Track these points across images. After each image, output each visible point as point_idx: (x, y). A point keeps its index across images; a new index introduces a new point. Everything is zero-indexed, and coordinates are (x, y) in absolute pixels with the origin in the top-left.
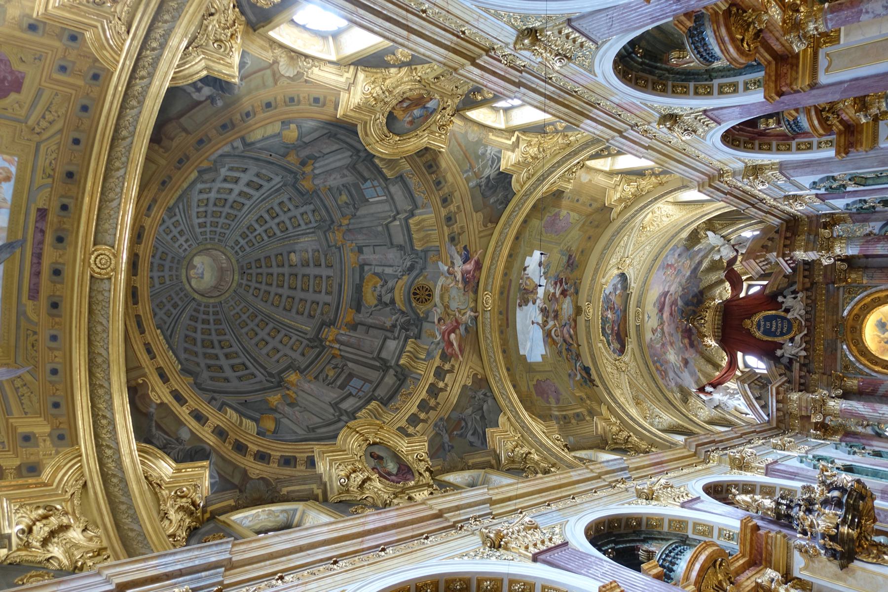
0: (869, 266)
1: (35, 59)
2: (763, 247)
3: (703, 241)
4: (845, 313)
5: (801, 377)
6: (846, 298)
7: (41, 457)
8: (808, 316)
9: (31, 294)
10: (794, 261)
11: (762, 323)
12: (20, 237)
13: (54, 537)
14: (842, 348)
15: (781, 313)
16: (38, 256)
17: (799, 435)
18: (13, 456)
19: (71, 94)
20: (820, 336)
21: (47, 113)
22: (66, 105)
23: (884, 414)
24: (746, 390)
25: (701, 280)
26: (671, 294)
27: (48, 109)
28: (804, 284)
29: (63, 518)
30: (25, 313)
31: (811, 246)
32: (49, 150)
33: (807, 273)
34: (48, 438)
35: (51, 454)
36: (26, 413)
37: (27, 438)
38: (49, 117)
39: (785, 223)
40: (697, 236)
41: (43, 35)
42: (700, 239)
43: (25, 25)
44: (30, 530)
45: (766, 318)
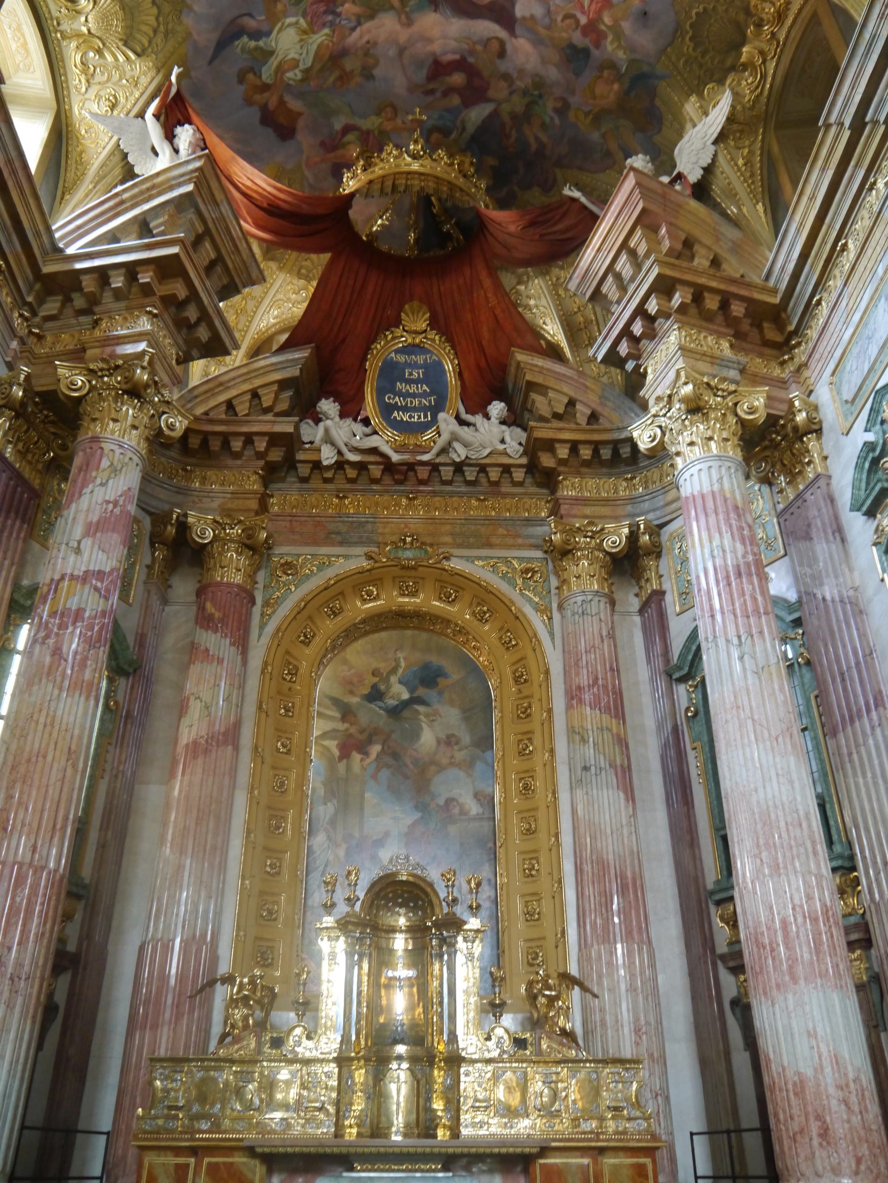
0: (615, 617)
2: (688, 244)
4: (455, 564)
5: (249, 439)
6: (506, 561)
8: (447, 472)
10: (636, 356)
11: (420, 359)
14: (346, 557)
17: (14, 344)
20: (387, 508)
23: (78, 551)
24: (172, 188)
26: (502, 53)
28: (549, 445)
31: (703, 366)
33: (586, 453)
39: (777, 300)
40: (711, 81)
42: (700, 95)
45: (433, 374)
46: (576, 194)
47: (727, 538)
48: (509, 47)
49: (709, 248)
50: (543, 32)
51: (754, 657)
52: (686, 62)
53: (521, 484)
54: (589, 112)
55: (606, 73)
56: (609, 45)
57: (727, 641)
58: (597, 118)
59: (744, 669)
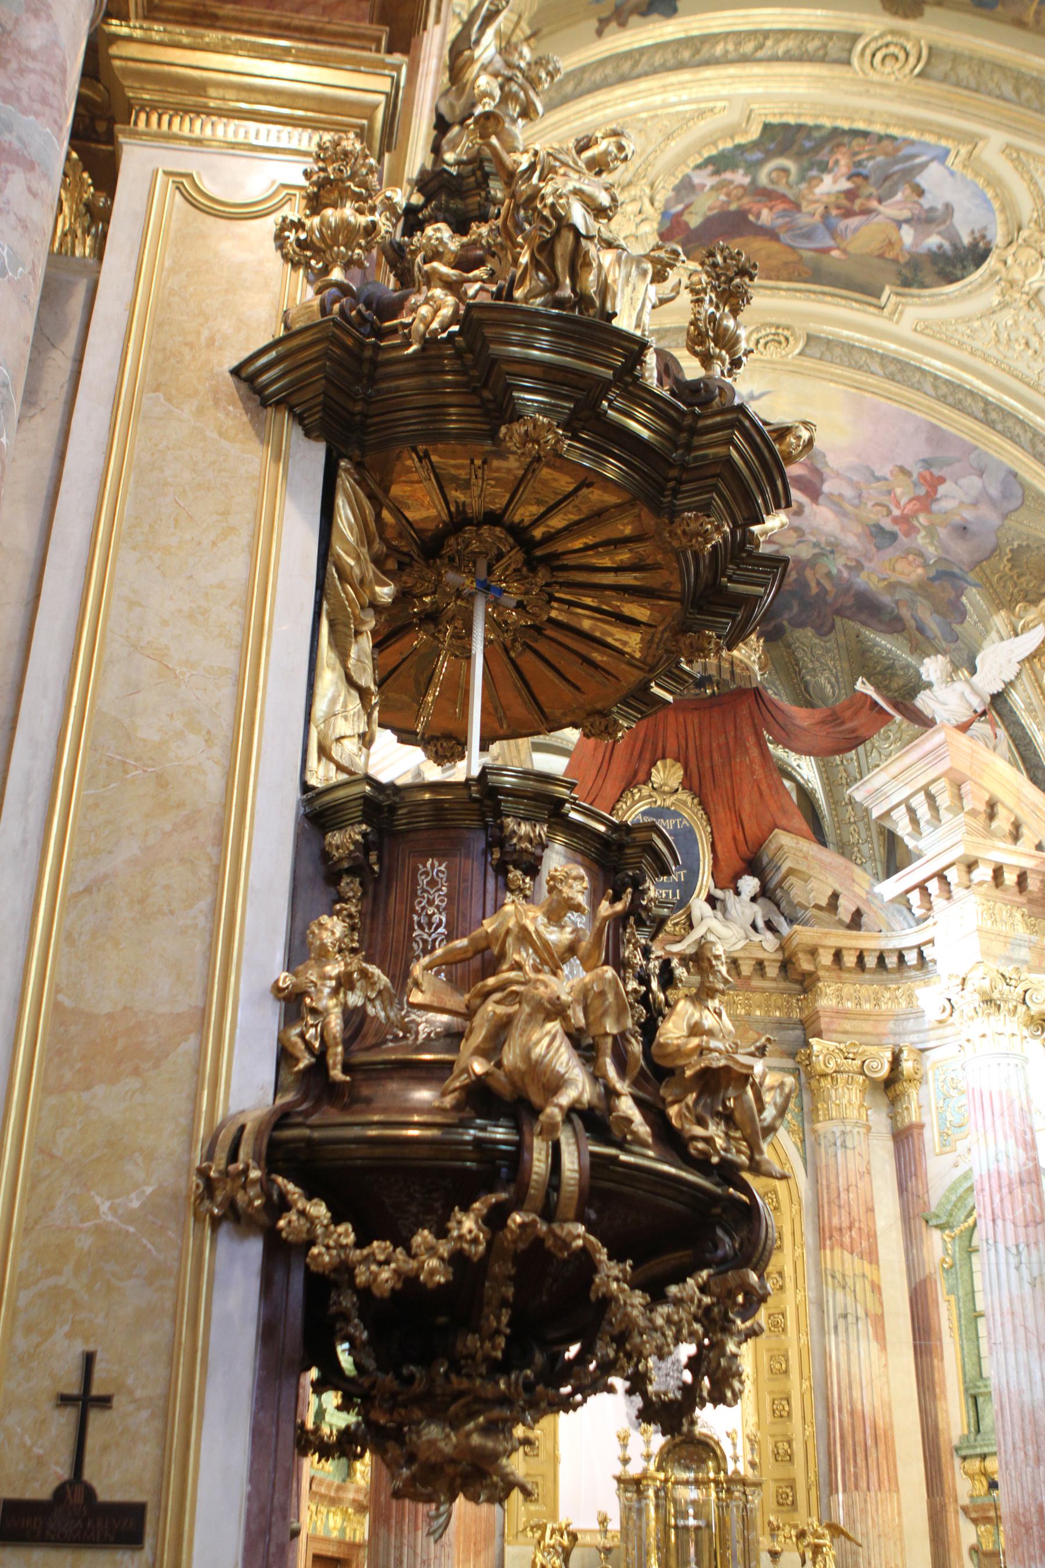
3: (1000, 620)
15: (705, 881)
25: (824, 630)
33: (850, 960)
42: (1011, 610)
46: (870, 691)
47: (1012, 1141)
48: (807, 510)
49: (1011, 811)
50: (849, 508)
51: (1030, 1269)
52: (1001, 578)
53: (774, 980)
54: (884, 579)
55: (911, 557)
56: (921, 539)
57: (1007, 1248)
58: (892, 587)
59: (1021, 1279)
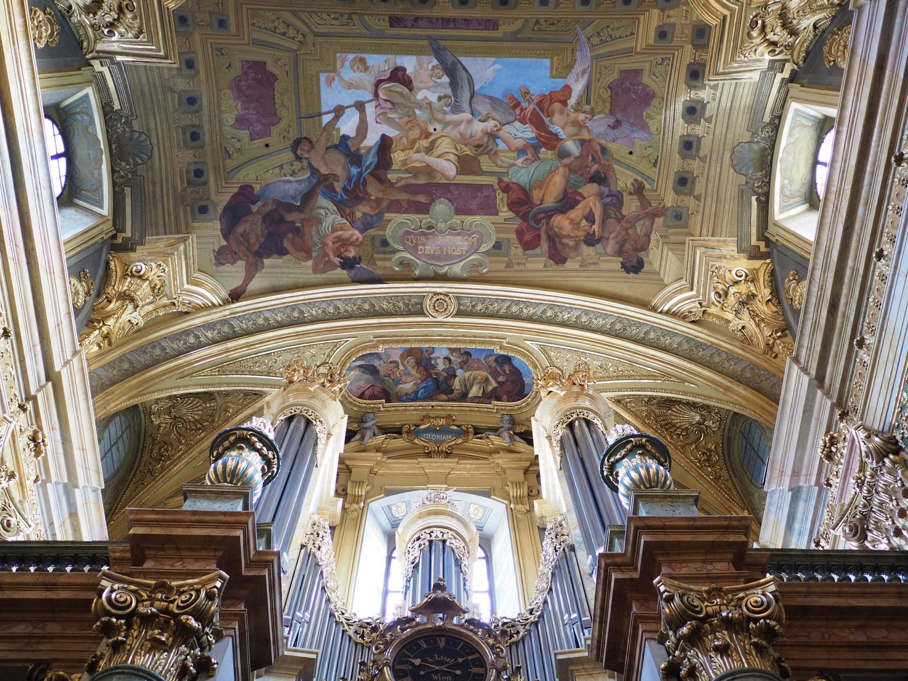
1: (222, 54)
7: (688, 22)
9: (491, 27)
12: (426, 42)
13: (791, 22)
16: (446, 22)
18: (680, 51)
19: (248, 9)
21: (278, 31)
22: (263, 12)
27: (274, 30)
29: (770, 10)
30: (514, 34)
32: (319, 22)
34: (667, 12)
35: (687, 11)
36: (632, 34)
37: (662, 34)
38: (282, 28)
41: (193, 52)
43: (191, 72)
44: (774, 44)
